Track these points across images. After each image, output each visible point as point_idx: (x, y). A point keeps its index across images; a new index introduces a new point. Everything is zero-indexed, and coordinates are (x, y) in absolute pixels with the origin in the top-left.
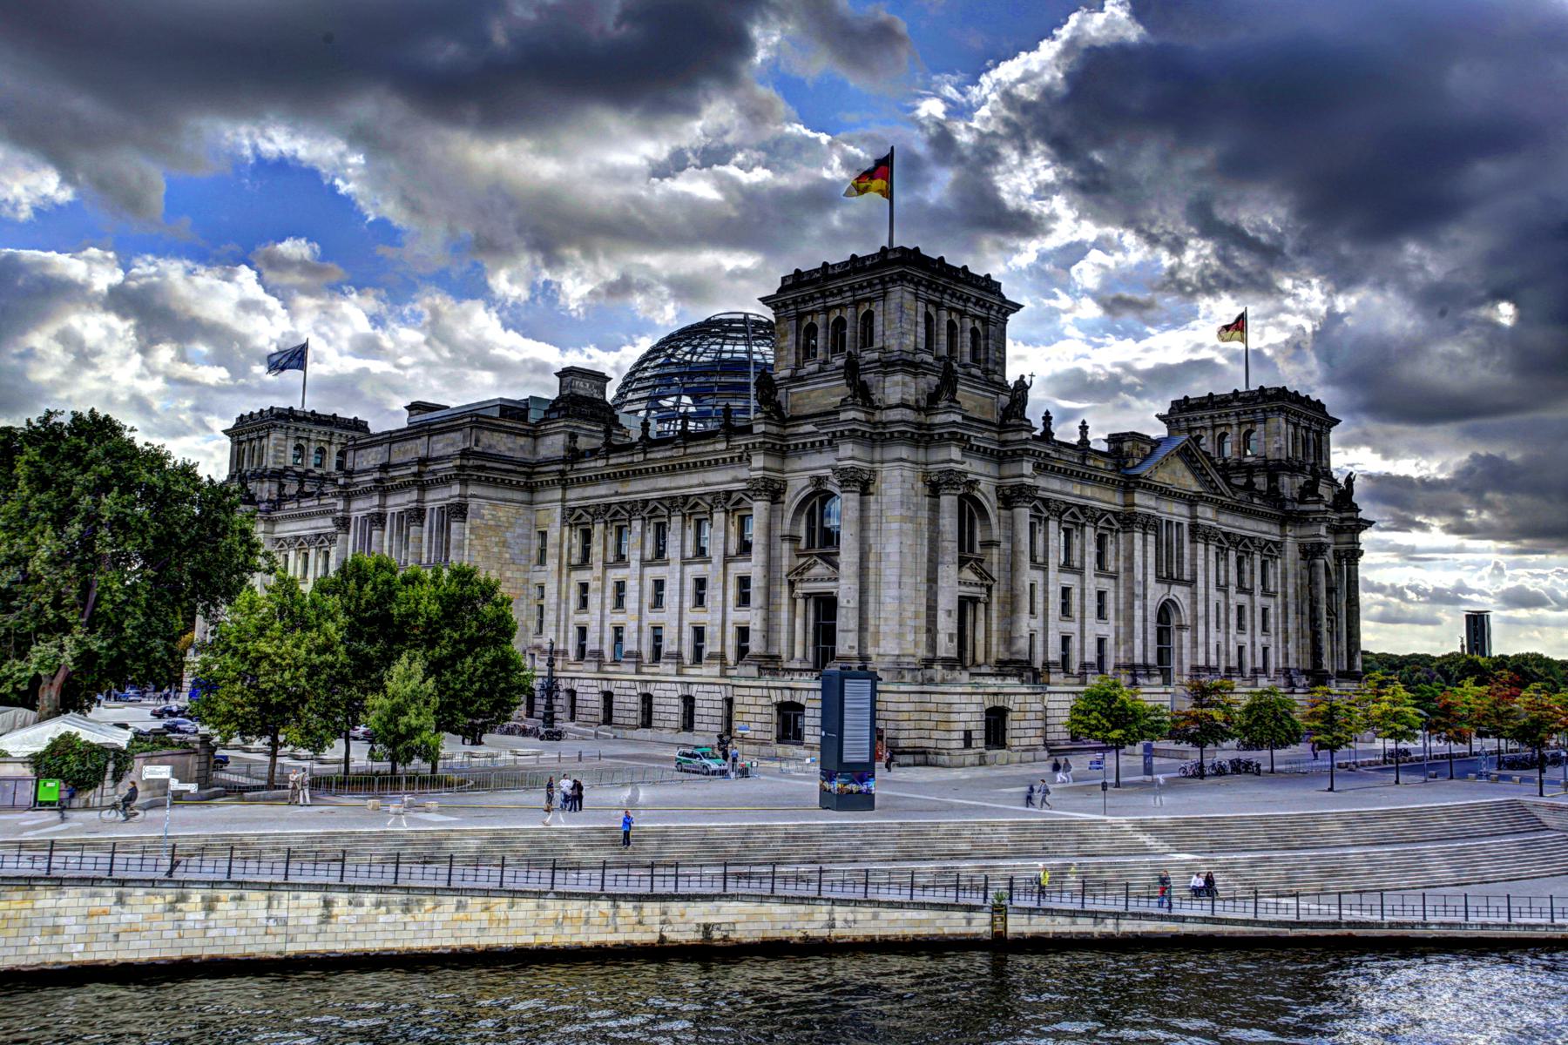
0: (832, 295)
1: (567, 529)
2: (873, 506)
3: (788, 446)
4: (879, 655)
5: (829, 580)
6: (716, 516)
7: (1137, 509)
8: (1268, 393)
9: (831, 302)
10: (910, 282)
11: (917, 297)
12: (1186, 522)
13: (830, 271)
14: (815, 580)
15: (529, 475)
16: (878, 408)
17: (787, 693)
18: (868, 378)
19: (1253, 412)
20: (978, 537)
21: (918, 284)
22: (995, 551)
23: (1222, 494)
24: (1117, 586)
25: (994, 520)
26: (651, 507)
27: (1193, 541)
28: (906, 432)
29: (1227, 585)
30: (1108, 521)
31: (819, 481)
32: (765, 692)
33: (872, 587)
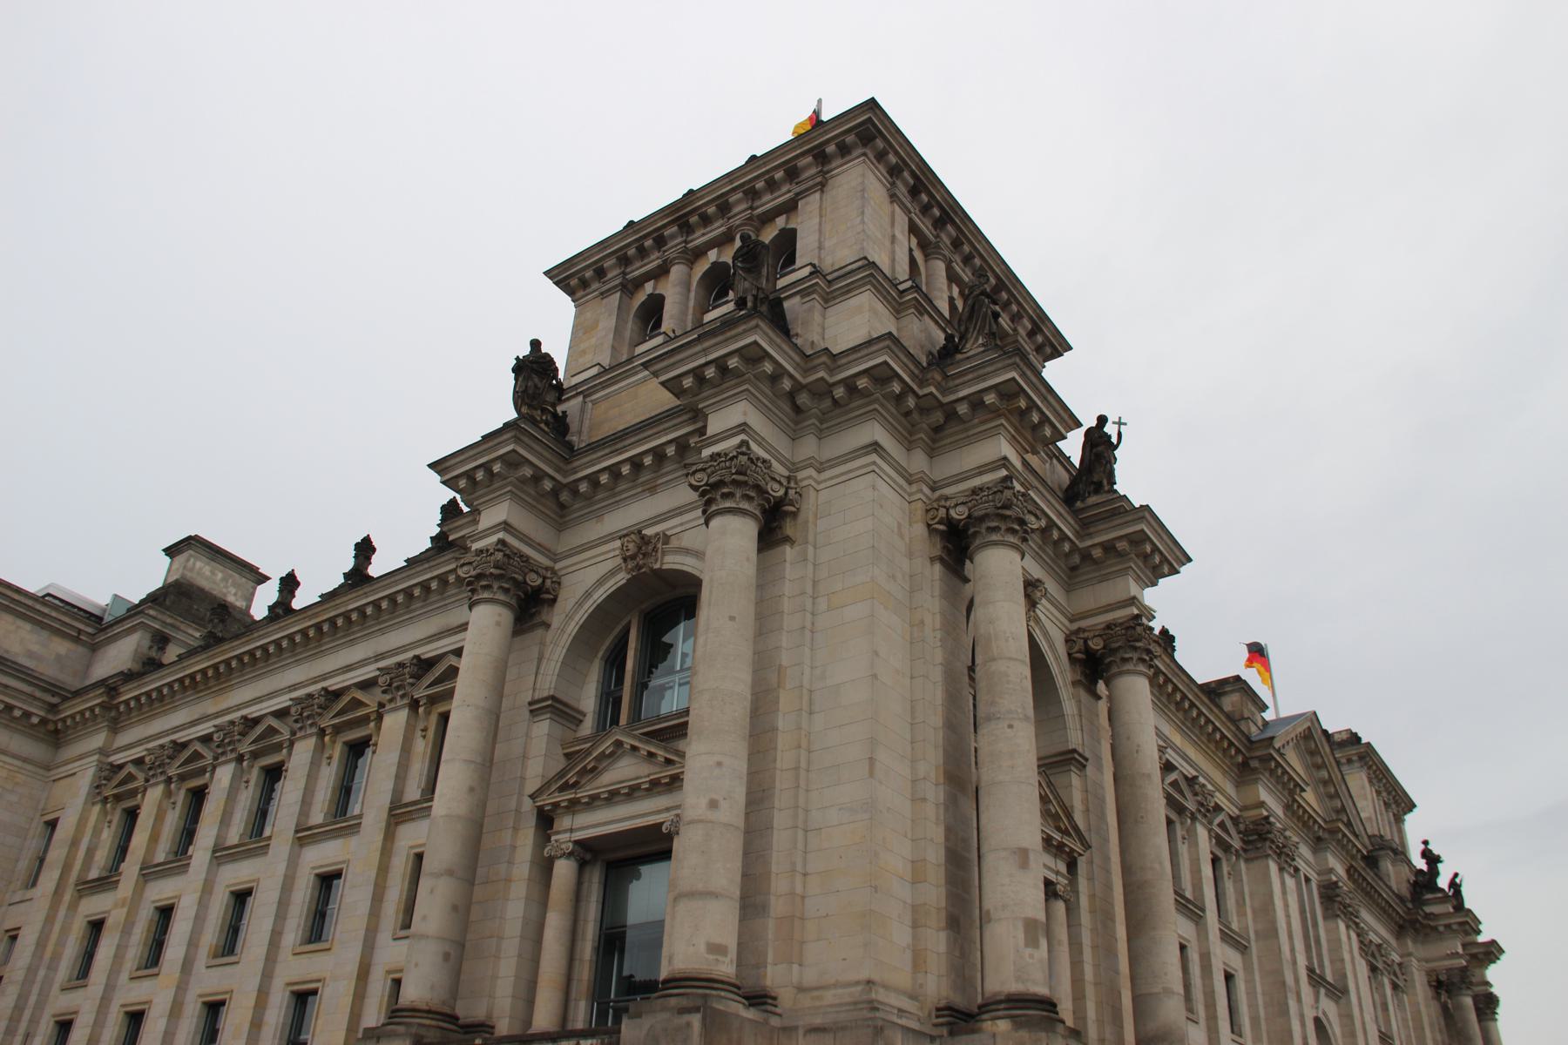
0: (706, 220)
1: (97, 808)
2: (790, 571)
3: (573, 489)
4: (801, 989)
5: (655, 787)
6: (388, 720)
8: (1337, 738)
9: (699, 238)
11: (893, 197)
12: (1313, 876)
14: (613, 797)
15: (53, 708)
21: (894, 172)
23: (1356, 836)
24: (1248, 968)
25: (1069, 707)
26: (259, 729)
27: (1330, 915)
30: (1222, 825)
31: (642, 545)
33: (782, 781)
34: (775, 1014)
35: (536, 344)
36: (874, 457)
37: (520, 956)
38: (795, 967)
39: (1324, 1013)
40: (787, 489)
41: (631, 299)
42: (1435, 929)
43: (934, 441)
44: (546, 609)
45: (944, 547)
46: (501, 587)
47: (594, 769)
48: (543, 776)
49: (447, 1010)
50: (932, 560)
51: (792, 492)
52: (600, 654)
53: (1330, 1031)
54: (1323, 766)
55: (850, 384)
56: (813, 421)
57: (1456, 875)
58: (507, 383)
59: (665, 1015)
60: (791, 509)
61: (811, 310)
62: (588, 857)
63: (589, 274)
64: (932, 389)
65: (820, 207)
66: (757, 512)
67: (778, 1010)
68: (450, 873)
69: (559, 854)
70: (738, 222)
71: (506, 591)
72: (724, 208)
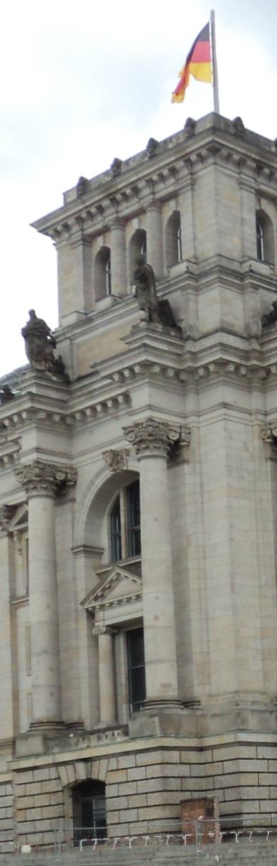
0: (126, 197)
4: (210, 696)
9: (127, 209)
10: (228, 158)
11: (241, 184)
13: (123, 169)
16: (189, 338)
17: (81, 767)
18: (175, 299)
21: (240, 163)
31: (116, 457)
32: (53, 773)
33: (193, 597)
34: (198, 709)
35: (32, 313)
36: (224, 411)
37: (90, 686)
38: (207, 686)
40: (180, 433)
41: (91, 247)
43: (264, 385)
44: (71, 489)
45: (273, 450)
46: (42, 487)
47: (109, 588)
48: (86, 589)
49: (58, 720)
50: (266, 459)
51: (183, 435)
52: (107, 512)
55: (206, 367)
56: (191, 386)
58: (20, 344)
59: (145, 718)
60: (186, 443)
61: (187, 301)
62: (116, 631)
63: (59, 228)
64: (255, 362)
65: (193, 204)
66: (165, 455)
67: (200, 707)
68: (45, 652)
69: (99, 633)
70: (146, 205)
71: (46, 488)
72: (136, 191)
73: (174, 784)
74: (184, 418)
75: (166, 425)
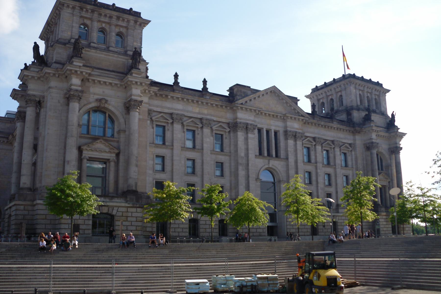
7: (238, 120)
8: (346, 77)
12: (281, 130)
19: (340, 86)
20: (116, 130)
22: (122, 135)
24: (230, 160)
25: (122, 120)
27: (286, 139)
28: (49, 73)
29: (316, 163)
36: (51, 90)
39: (274, 166)
40: (40, 98)
42: (365, 132)
53: (277, 170)
54: (282, 99)
57: (393, 112)
73: (20, 217)
74: (43, 93)
75: (34, 95)
